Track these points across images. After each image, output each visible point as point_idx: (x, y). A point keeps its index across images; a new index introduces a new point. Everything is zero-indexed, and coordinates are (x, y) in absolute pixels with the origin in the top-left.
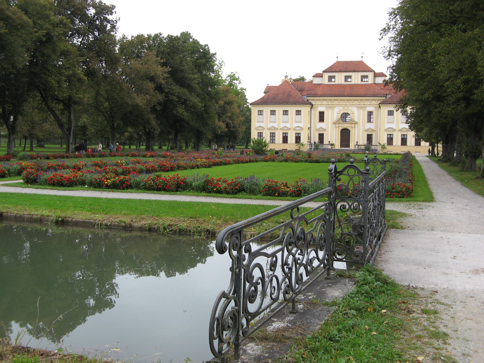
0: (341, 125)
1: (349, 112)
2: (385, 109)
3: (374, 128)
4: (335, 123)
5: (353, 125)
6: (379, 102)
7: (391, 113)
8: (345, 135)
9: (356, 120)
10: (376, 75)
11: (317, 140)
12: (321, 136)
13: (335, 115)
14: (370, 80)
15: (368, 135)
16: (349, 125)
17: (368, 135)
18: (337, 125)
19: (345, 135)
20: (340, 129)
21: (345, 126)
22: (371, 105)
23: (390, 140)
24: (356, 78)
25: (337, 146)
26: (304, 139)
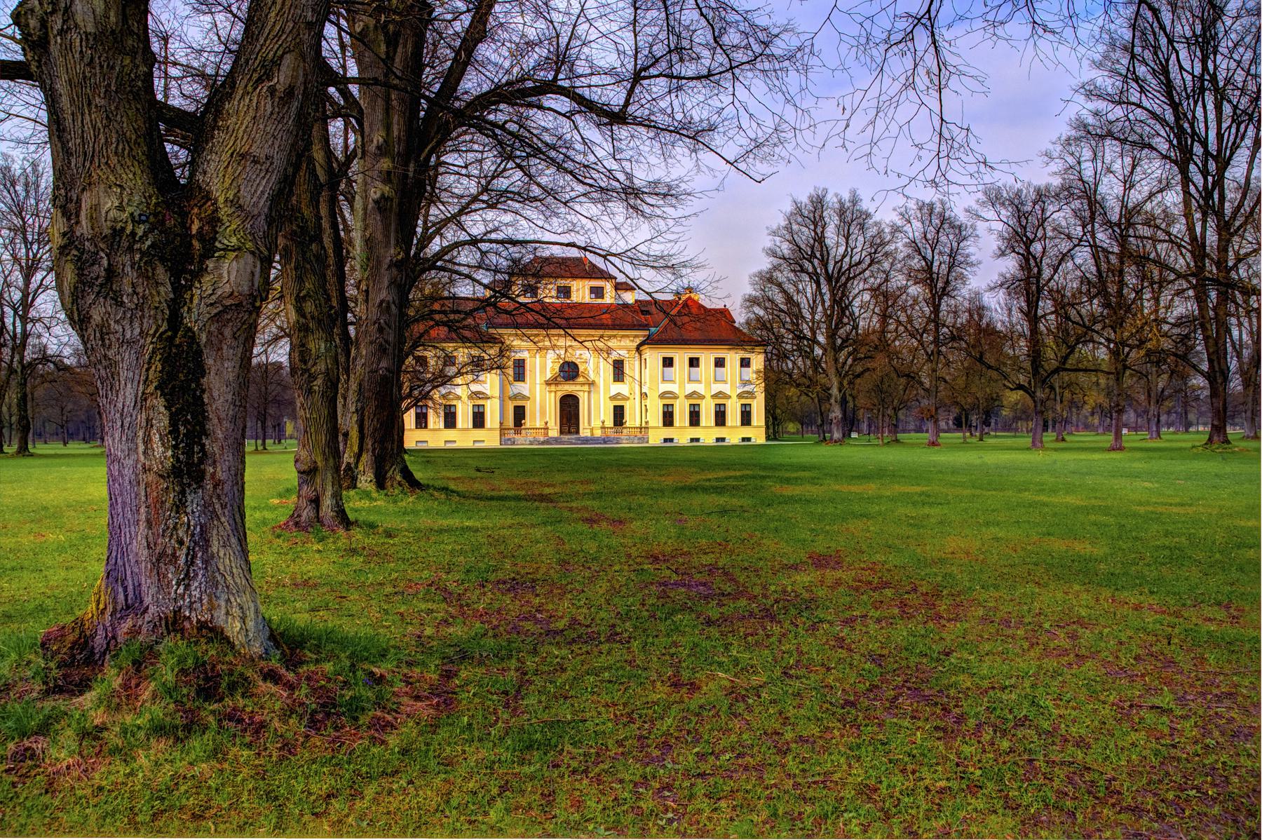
0: (560, 387)
1: (577, 362)
2: (654, 356)
3: (627, 394)
4: (548, 383)
5: (586, 388)
6: (638, 341)
7: (668, 362)
8: (569, 410)
9: (592, 376)
10: (619, 287)
11: (610, 422)
12: (520, 413)
13: (549, 365)
14: (609, 298)
15: (615, 407)
16: (578, 388)
17: (615, 407)
18: (553, 388)
19: (569, 410)
20: (560, 394)
21: (569, 388)
22: (623, 344)
23: (668, 419)
24: (581, 292)
25: (554, 432)
26: (492, 419)
